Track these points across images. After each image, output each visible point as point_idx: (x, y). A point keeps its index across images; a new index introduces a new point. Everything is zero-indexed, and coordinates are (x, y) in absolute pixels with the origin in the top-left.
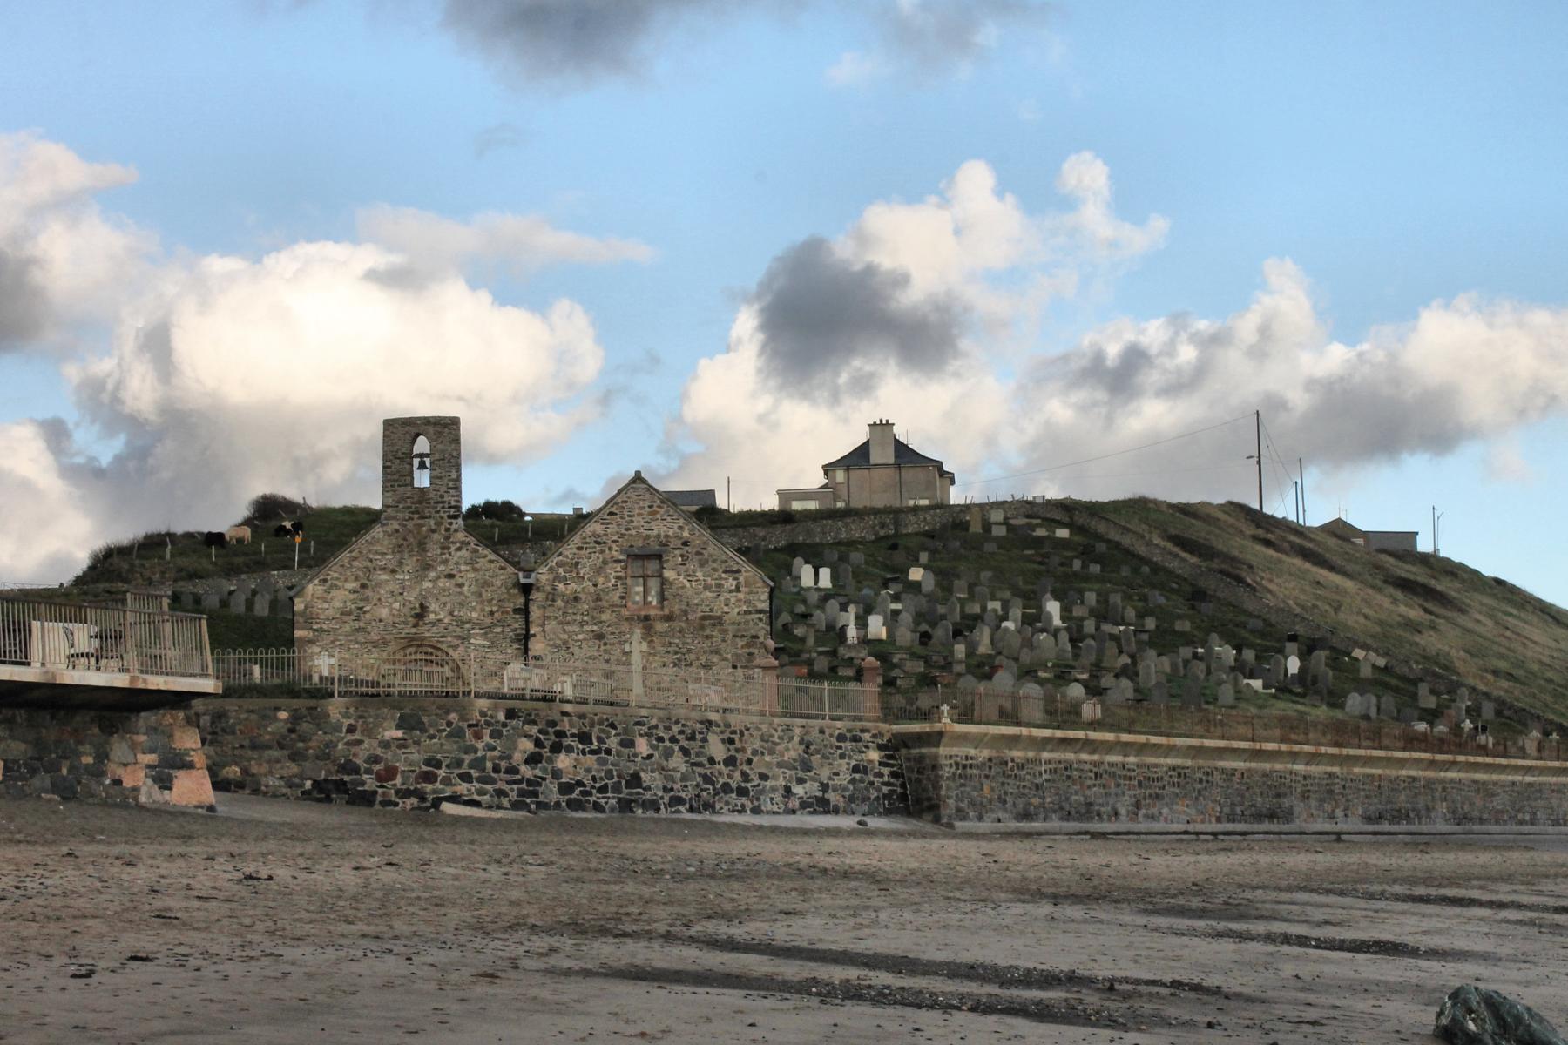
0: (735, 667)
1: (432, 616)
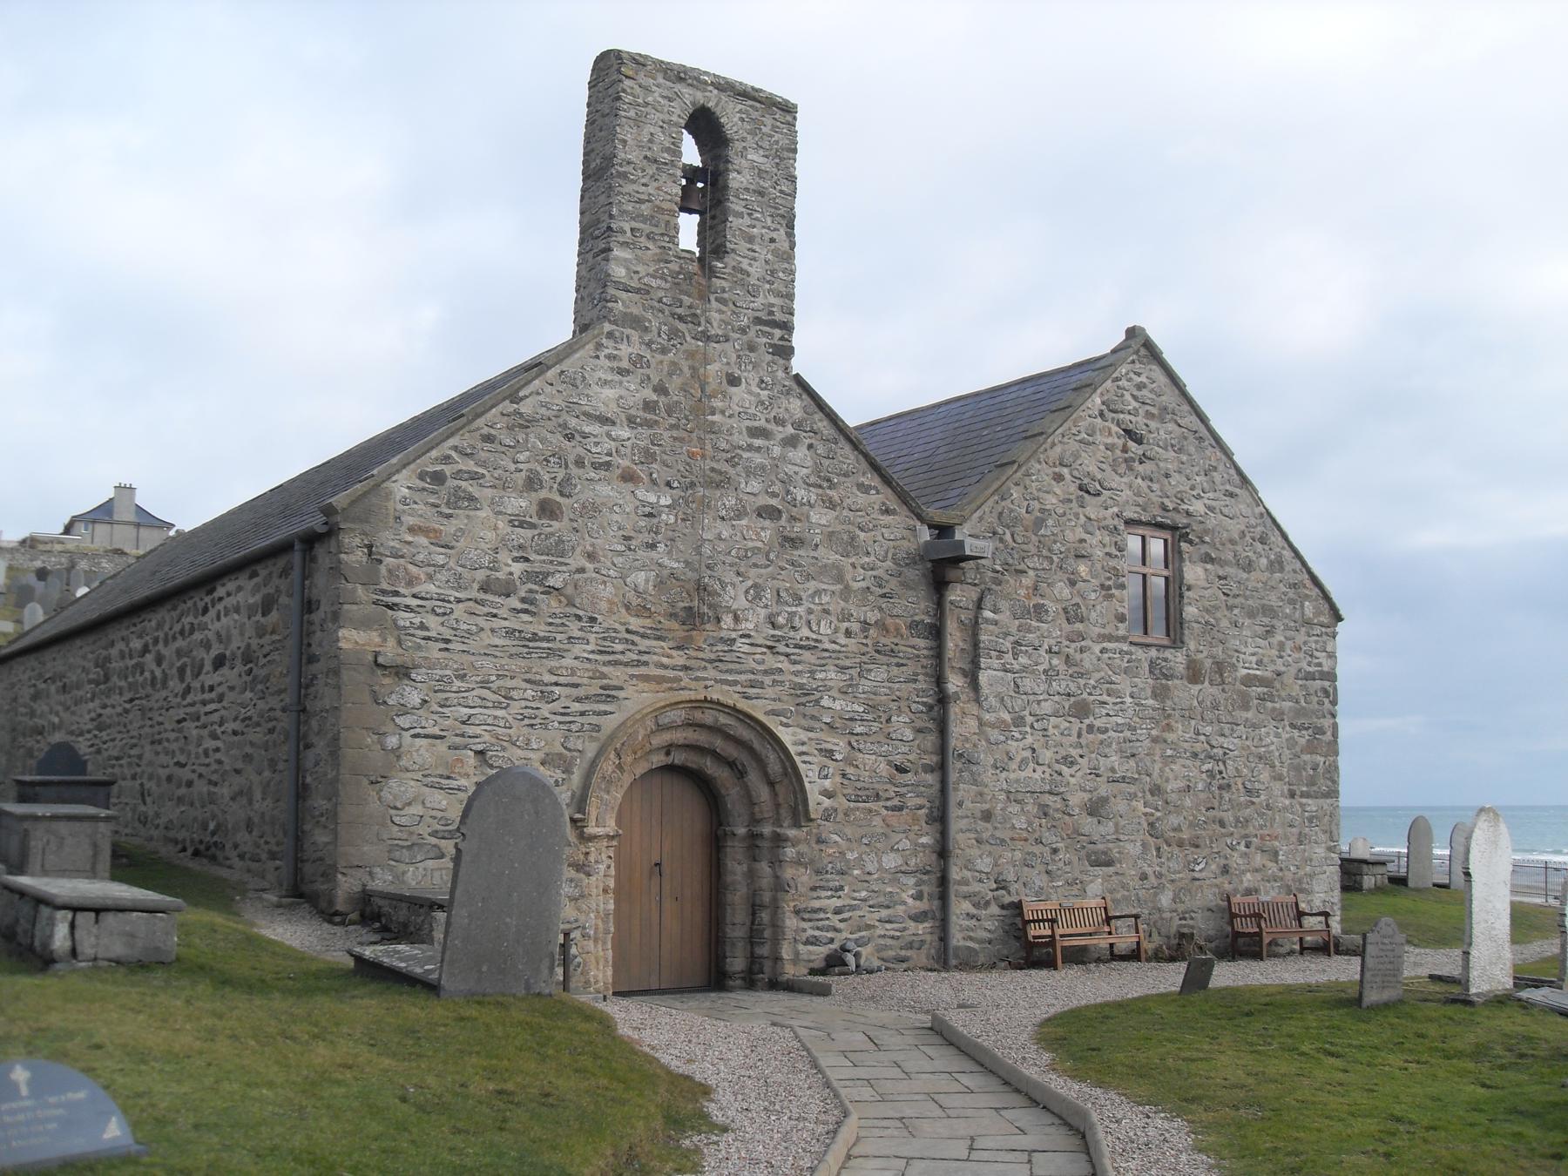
0: (1292, 795)
1: (728, 620)
